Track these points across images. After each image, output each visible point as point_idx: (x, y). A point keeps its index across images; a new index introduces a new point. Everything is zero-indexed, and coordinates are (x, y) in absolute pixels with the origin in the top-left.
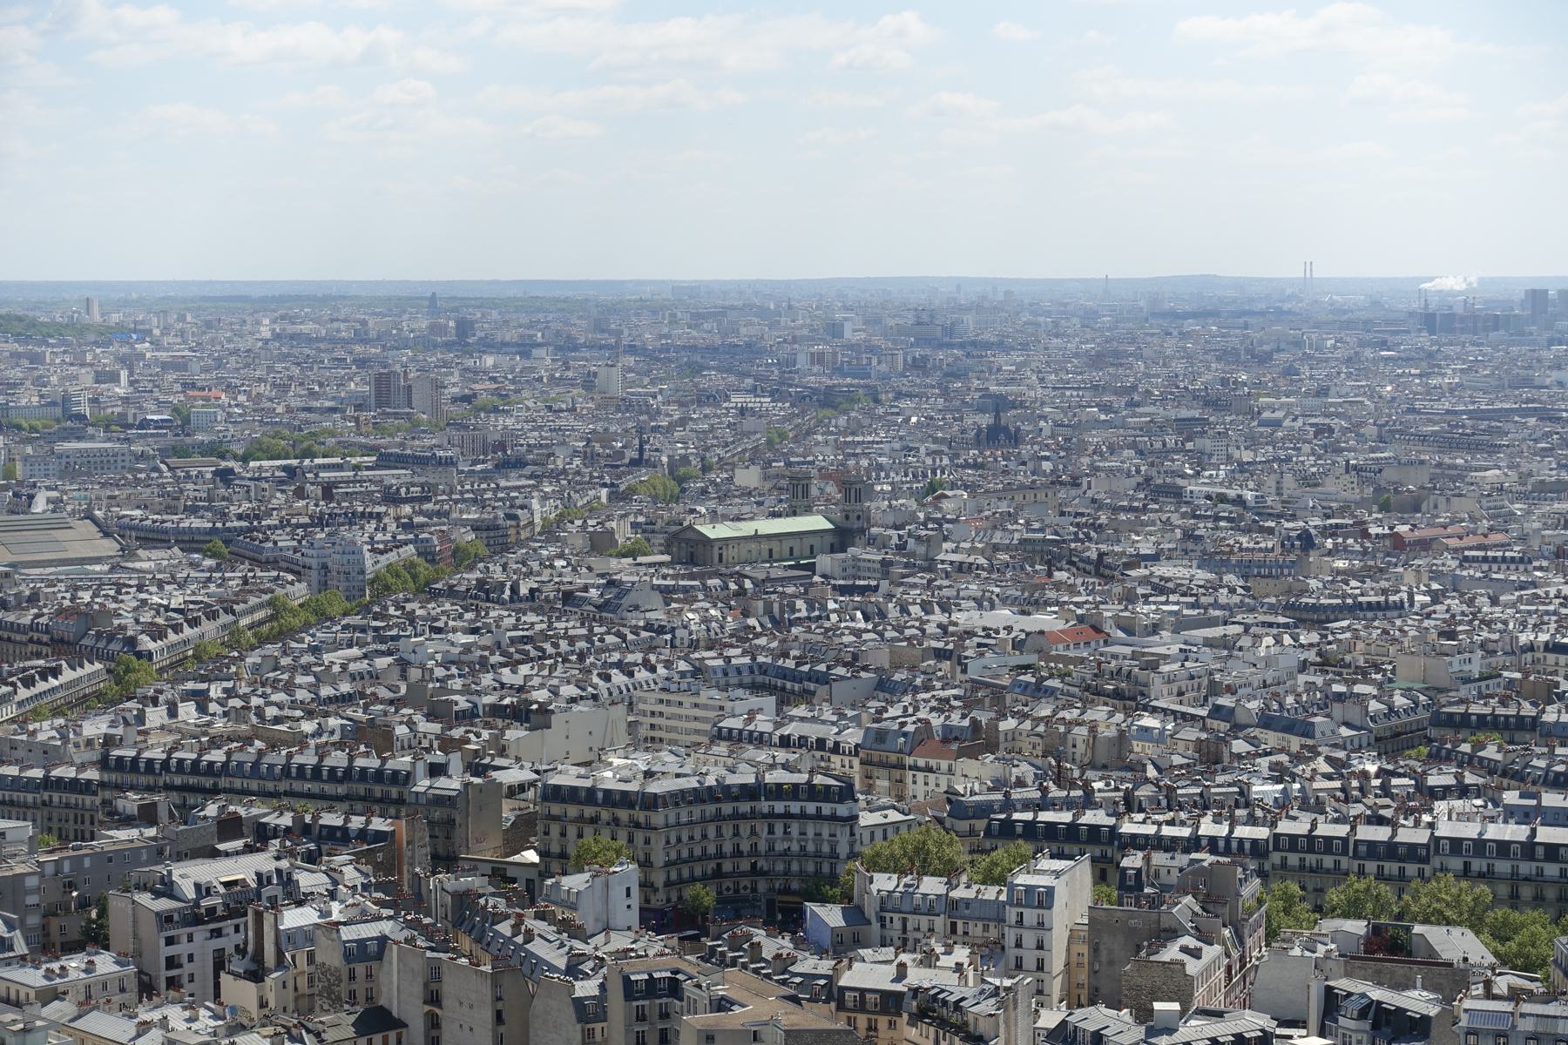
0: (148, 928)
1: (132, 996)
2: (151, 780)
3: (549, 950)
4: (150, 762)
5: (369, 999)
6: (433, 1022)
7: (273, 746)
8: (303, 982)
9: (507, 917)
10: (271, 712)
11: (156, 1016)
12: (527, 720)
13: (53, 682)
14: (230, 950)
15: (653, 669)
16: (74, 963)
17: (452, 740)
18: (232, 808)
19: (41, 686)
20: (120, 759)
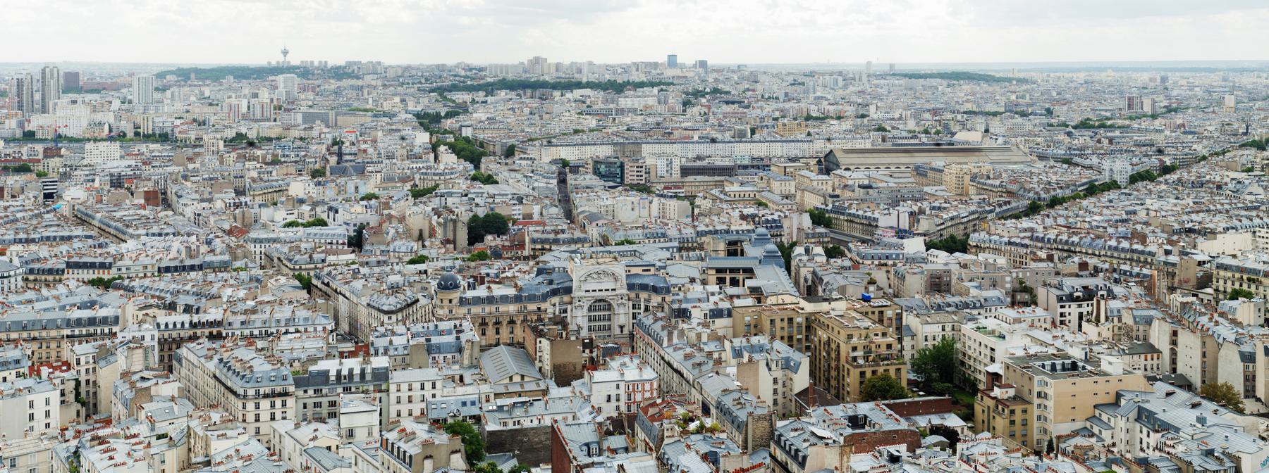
0: (1053, 299)
1: (1048, 326)
2: (1049, 246)
3: (1225, 331)
4: (1049, 239)
5: (1145, 339)
6: (1174, 353)
7: (1098, 237)
8: (1116, 329)
9: (1205, 314)
10: (1094, 224)
11: (1060, 334)
12: (1205, 235)
13: (1008, 207)
14: (1085, 313)
15: (1262, 219)
16: (1028, 309)
17: (1172, 241)
18: (1084, 259)
19: (1004, 208)
20: (1037, 237)
